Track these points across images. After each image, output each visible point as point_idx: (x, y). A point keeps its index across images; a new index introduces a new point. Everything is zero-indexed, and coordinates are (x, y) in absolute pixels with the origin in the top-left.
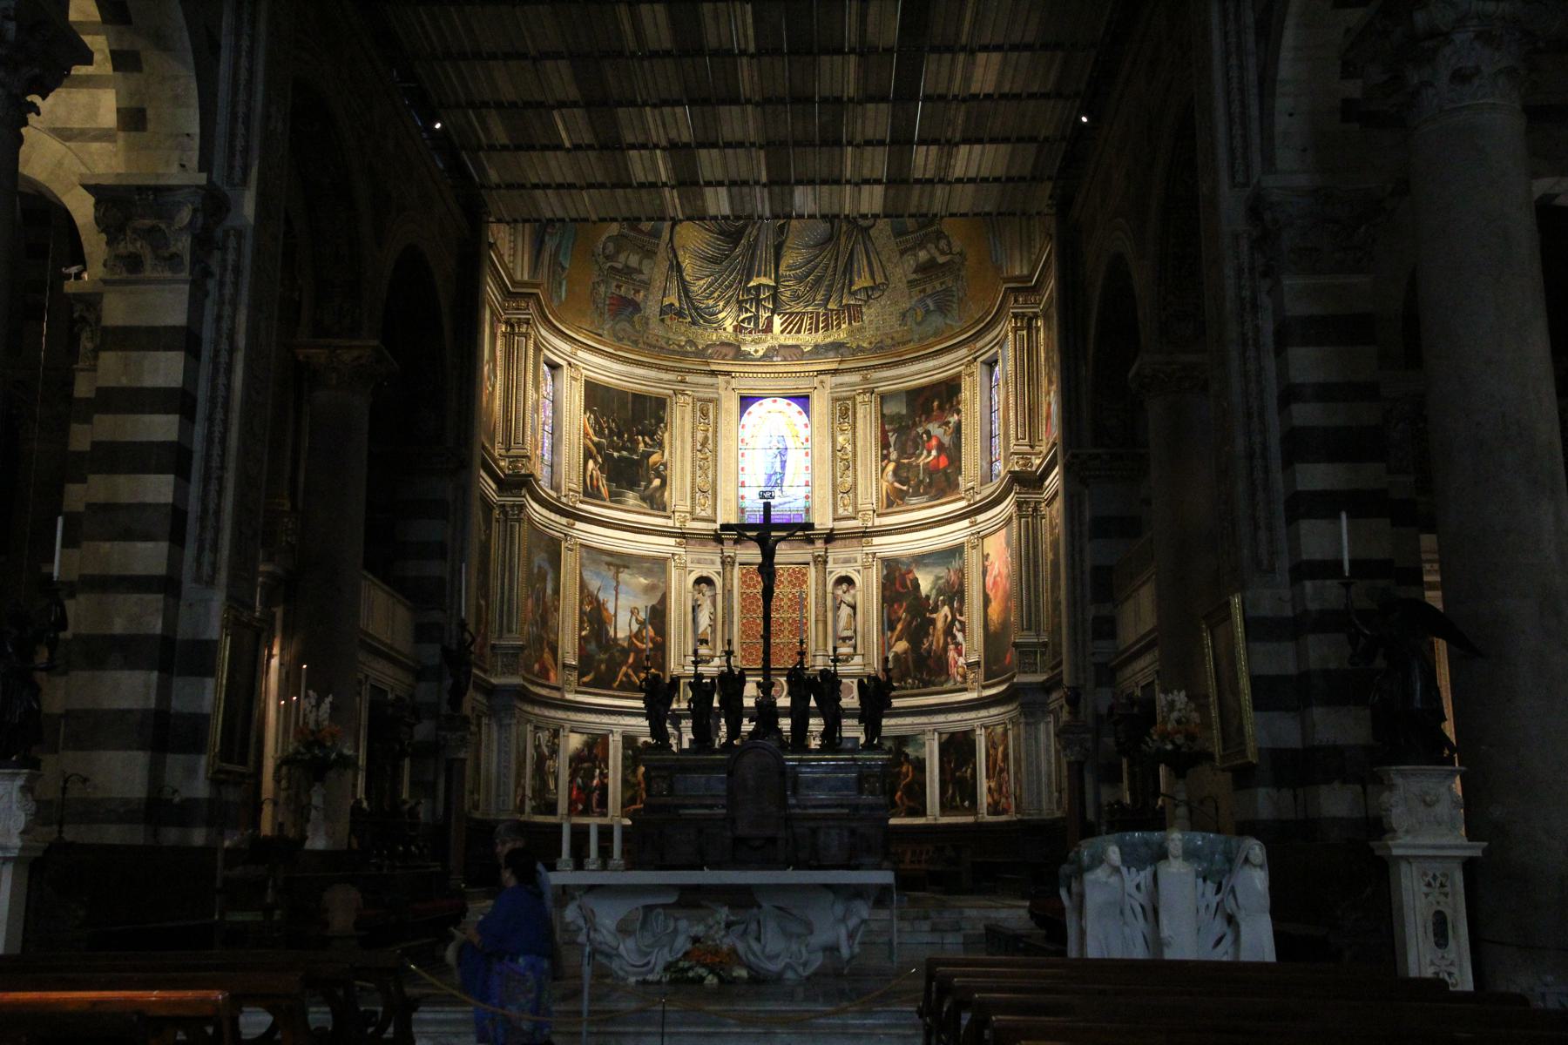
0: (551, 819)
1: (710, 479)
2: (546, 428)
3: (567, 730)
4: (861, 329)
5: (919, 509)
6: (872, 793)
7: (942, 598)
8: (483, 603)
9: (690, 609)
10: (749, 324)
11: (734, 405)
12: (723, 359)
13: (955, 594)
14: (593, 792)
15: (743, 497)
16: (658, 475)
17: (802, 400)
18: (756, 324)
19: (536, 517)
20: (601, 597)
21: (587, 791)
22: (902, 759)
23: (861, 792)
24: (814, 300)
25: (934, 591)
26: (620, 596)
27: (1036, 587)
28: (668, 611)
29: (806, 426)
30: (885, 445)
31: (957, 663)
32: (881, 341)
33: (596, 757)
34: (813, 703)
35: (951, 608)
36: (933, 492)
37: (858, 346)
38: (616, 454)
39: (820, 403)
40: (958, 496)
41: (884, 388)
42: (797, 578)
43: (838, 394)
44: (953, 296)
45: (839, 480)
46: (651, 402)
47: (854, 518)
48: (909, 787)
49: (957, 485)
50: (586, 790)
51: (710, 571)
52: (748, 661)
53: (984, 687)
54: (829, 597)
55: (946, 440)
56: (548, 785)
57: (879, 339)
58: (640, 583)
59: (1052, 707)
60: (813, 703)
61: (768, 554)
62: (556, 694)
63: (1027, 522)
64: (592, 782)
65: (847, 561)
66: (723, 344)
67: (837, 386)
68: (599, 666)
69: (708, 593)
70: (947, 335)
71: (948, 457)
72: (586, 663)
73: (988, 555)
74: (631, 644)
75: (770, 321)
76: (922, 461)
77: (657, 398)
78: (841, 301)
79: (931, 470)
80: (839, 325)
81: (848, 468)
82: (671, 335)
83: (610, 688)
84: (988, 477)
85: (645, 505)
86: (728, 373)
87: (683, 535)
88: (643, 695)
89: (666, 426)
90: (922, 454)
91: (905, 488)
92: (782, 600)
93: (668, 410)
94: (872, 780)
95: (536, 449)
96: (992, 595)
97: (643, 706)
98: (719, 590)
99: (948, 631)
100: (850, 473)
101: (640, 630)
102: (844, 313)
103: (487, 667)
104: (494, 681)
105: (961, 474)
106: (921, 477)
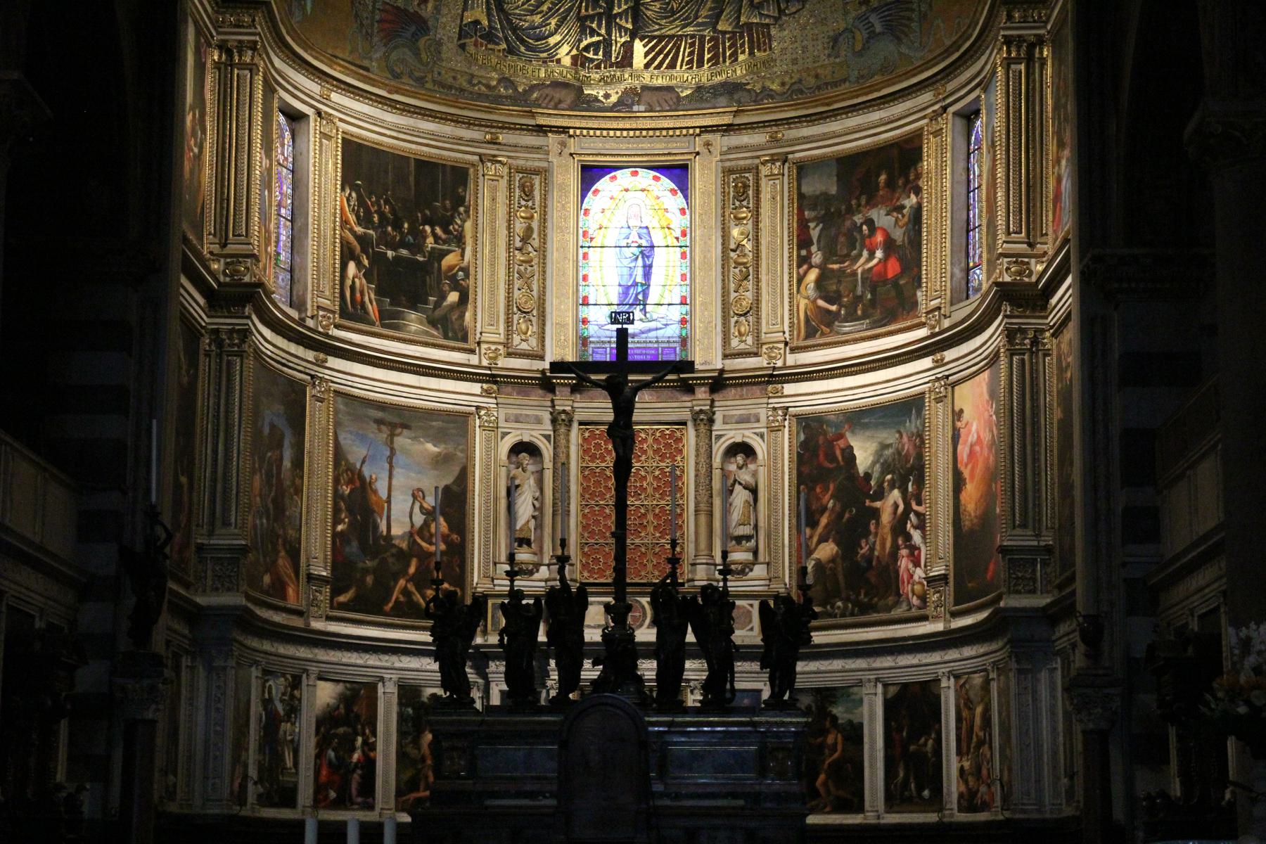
0: (286, 814)
1: (535, 293)
2: (283, 211)
3: (313, 676)
4: (766, 63)
5: (856, 341)
6: (781, 775)
7: (889, 477)
8: (184, 480)
9: (503, 492)
10: (596, 53)
11: (572, 179)
12: (555, 108)
13: (910, 471)
14: (354, 771)
15: (585, 321)
16: (456, 286)
17: (677, 171)
18: (607, 54)
19: (267, 349)
20: (366, 472)
22: (828, 724)
23: (763, 772)
24: (696, 17)
25: (878, 467)
26: (397, 471)
28: (469, 495)
29: (683, 212)
30: (804, 242)
31: (911, 576)
32: (800, 81)
33: (357, 717)
34: (690, 637)
36: (877, 314)
37: (764, 88)
38: (390, 254)
39: (704, 177)
40: (916, 321)
41: (803, 153)
42: (668, 446)
43: (733, 163)
44: (913, 10)
45: (733, 295)
46: (444, 173)
47: (756, 355)
48: (836, 769)
49: (915, 304)
50: (341, 769)
51: (533, 433)
52: (591, 571)
53: (955, 615)
54: (717, 474)
55: (898, 235)
56: (284, 761)
57: (796, 77)
58: (426, 450)
59: (1060, 645)
60: (690, 637)
61: (624, 408)
62: (297, 622)
63: (1023, 360)
64: (351, 757)
65: (744, 420)
66: (557, 85)
67: (731, 150)
68: (363, 580)
69: (531, 468)
70: (901, 71)
71: (900, 260)
72: (342, 574)
73: (961, 411)
75: (629, 48)
76: (862, 265)
77: (453, 168)
78: (738, 18)
79: (874, 281)
80: (734, 56)
81: (746, 278)
82: (475, 70)
83: (380, 612)
84: (963, 291)
86: (564, 130)
87: (492, 379)
88: (430, 623)
89: (467, 212)
90: (860, 255)
91: (834, 308)
92: (644, 478)
93: (471, 186)
94: (780, 756)
95: (268, 243)
96: (966, 473)
97: (430, 639)
98: (548, 463)
99: (899, 528)
100: (750, 285)
101: (426, 524)
102: (742, 37)
103: (191, 579)
104: (201, 600)
105: (920, 286)
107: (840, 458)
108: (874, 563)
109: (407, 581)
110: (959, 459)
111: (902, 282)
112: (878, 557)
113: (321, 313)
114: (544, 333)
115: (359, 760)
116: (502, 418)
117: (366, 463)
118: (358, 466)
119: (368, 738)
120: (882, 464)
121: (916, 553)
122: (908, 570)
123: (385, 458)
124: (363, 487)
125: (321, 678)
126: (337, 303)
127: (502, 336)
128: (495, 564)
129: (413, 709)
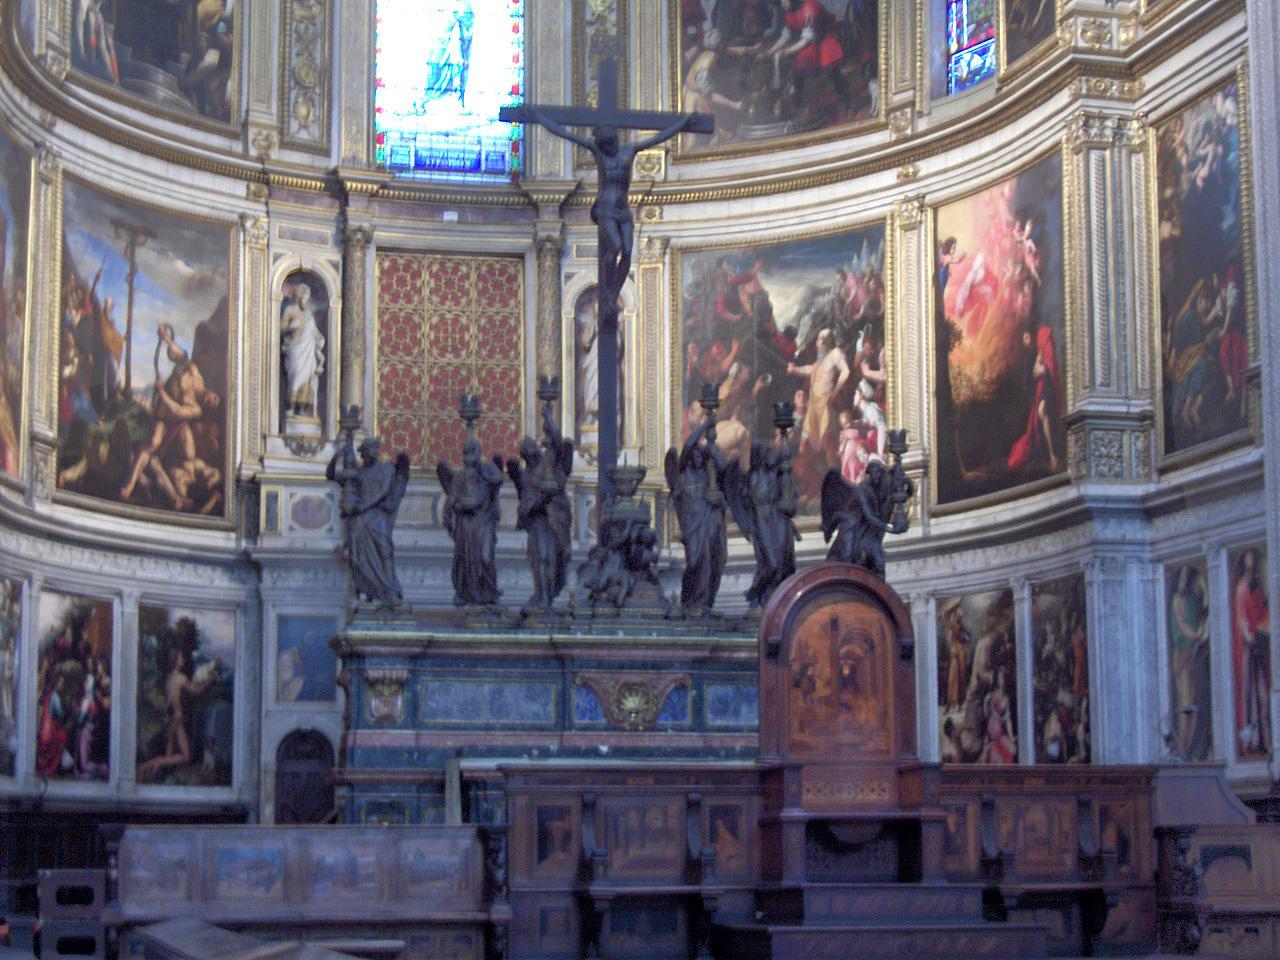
1: (318, 62)
3: (37, 585)
5: (771, 149)
7: (825, 333)
13: (861, 324)
14: (83, 725)
15: (379, 110)
16: (216, 42)
20: (101, 294)
21: (69, 725)
25: (807, 320)
26: (139, 297)
27: (1120, 295)
33: (88, 648)
35: (850, 356)
40: (873, 122)
64: (79, 704)
68: (96, 450)
74: (158, 403)
76: (781, 48)
79: (798, 70)
85: (189, 104)
90: (777, 36)
91: (738, 105)
96: (962, 324)
101: (175, 377)
106: (776, 82)
107: (747, 307)
108: (801, 449)
109: (152, 455)
110: (947, 305)
111: (844, 71)
112: (808, 442)
113: (51, 53)
114: (330, 118)
115: (89, 711)
116: (275, 232)
117: (101, 280)
118: (91, 283)
119: (101, 677)
120: (815, 317)
121: (869, 434)
122: (856, 458)
123: (123, 277)
124: (96, 316)
125: (45, 589)
126: (68, 43)
127: (275, 118)
128: (264, 437)
129: (159, 638)
